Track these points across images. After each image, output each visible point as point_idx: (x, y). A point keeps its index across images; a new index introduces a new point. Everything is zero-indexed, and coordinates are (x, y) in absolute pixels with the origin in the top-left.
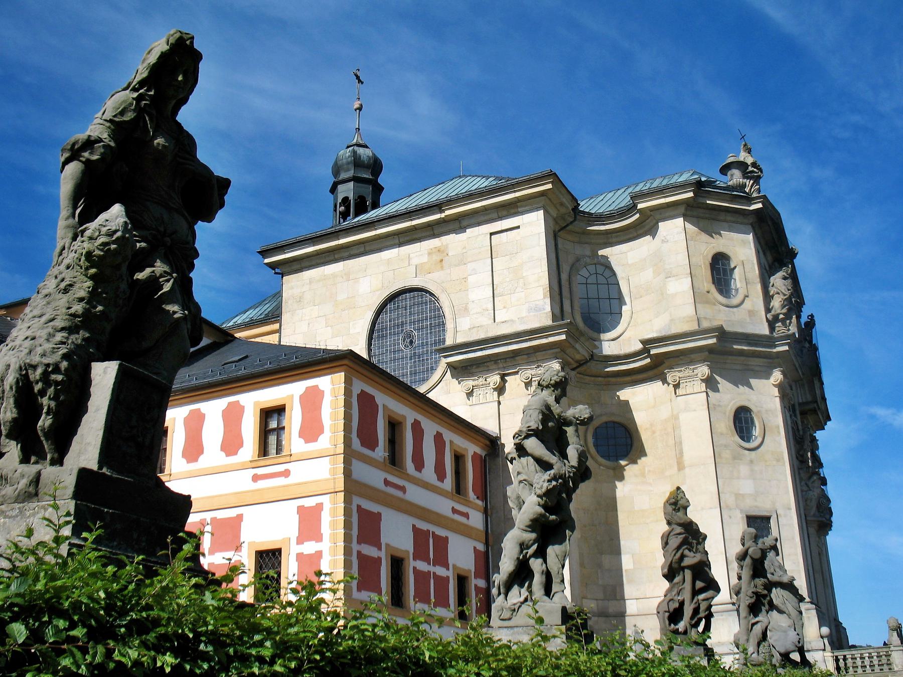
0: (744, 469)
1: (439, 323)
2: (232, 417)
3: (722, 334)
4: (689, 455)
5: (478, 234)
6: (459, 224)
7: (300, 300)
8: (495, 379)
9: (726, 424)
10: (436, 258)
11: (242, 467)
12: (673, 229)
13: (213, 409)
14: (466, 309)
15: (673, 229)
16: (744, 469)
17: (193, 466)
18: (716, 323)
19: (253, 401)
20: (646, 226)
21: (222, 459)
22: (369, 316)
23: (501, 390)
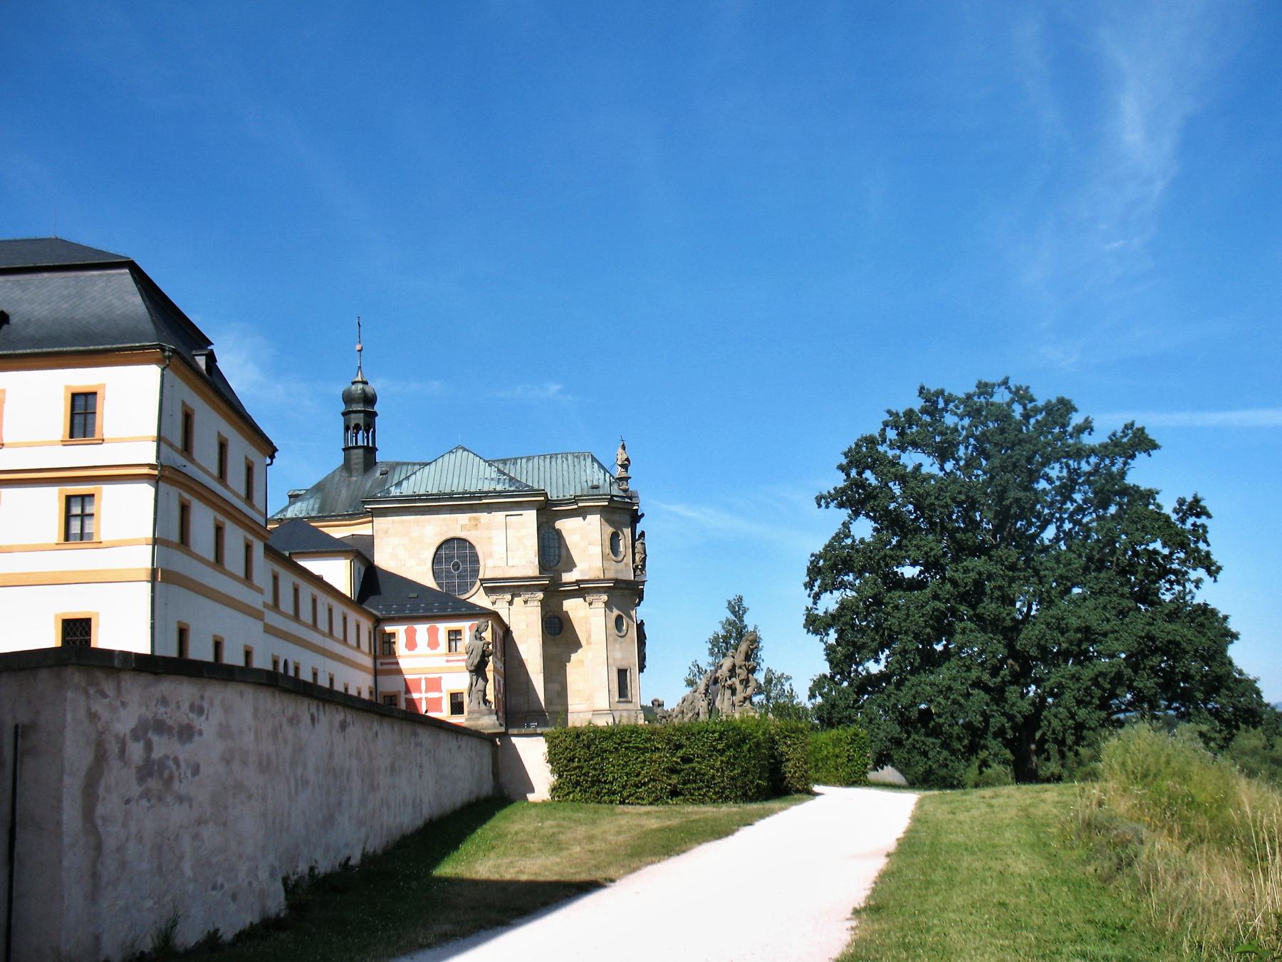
0: (618, 646)
1: (475, 559)
2: (433, 634)
3: (617, 581)
4: (593, 638)
5: (499, 516)
6: (489, 508)
7: (386, 532)
8: (508, 597)
9: (612, 623)
10: (473, 523)
11: (441, 655)
12: (594, 520)
13: (422, 629)
14: (491, 556)
15: (594, 520)
16: (618, 646)
17: (411, 653)
18: (611, 574)
19: (443, 627)
20: (582, 513)
21: (428, 651)
22: (433, 550)
23: (511, 603)
